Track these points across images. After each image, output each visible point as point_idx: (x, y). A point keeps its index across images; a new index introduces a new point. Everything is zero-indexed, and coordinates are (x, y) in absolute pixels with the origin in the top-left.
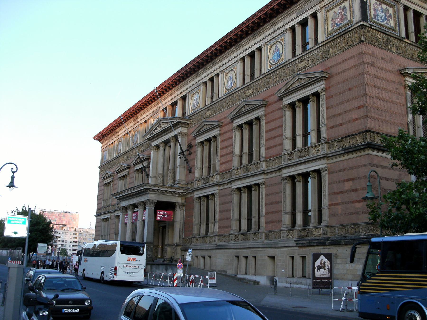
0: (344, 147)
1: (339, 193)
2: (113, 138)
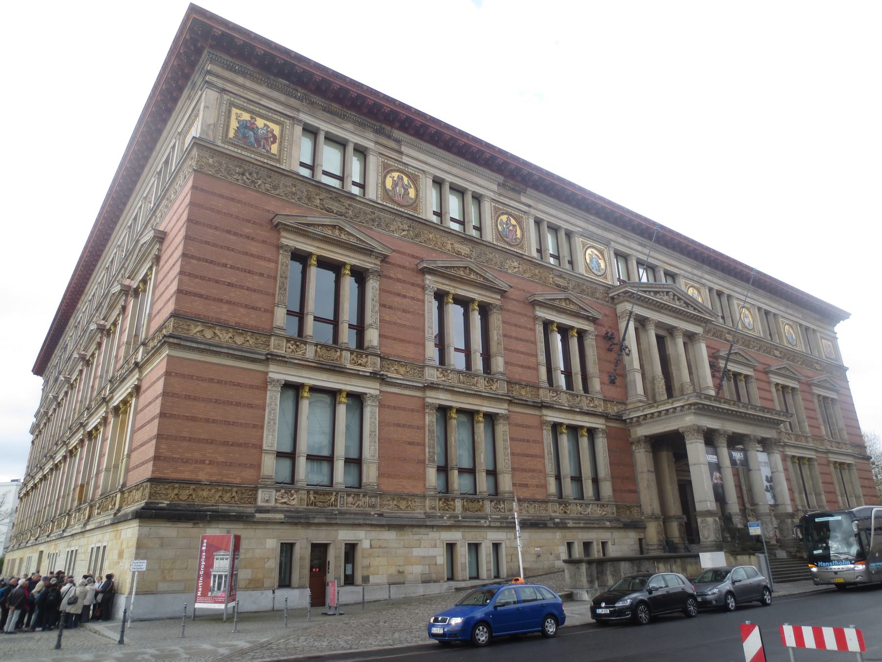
2: (349, 126)
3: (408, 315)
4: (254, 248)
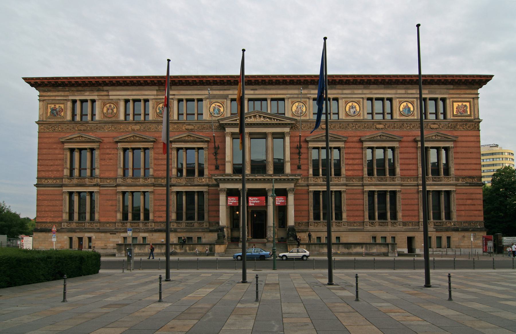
1: (463, 205)
2: (87, 93)
3: (111, 161)
4: (57, 151)
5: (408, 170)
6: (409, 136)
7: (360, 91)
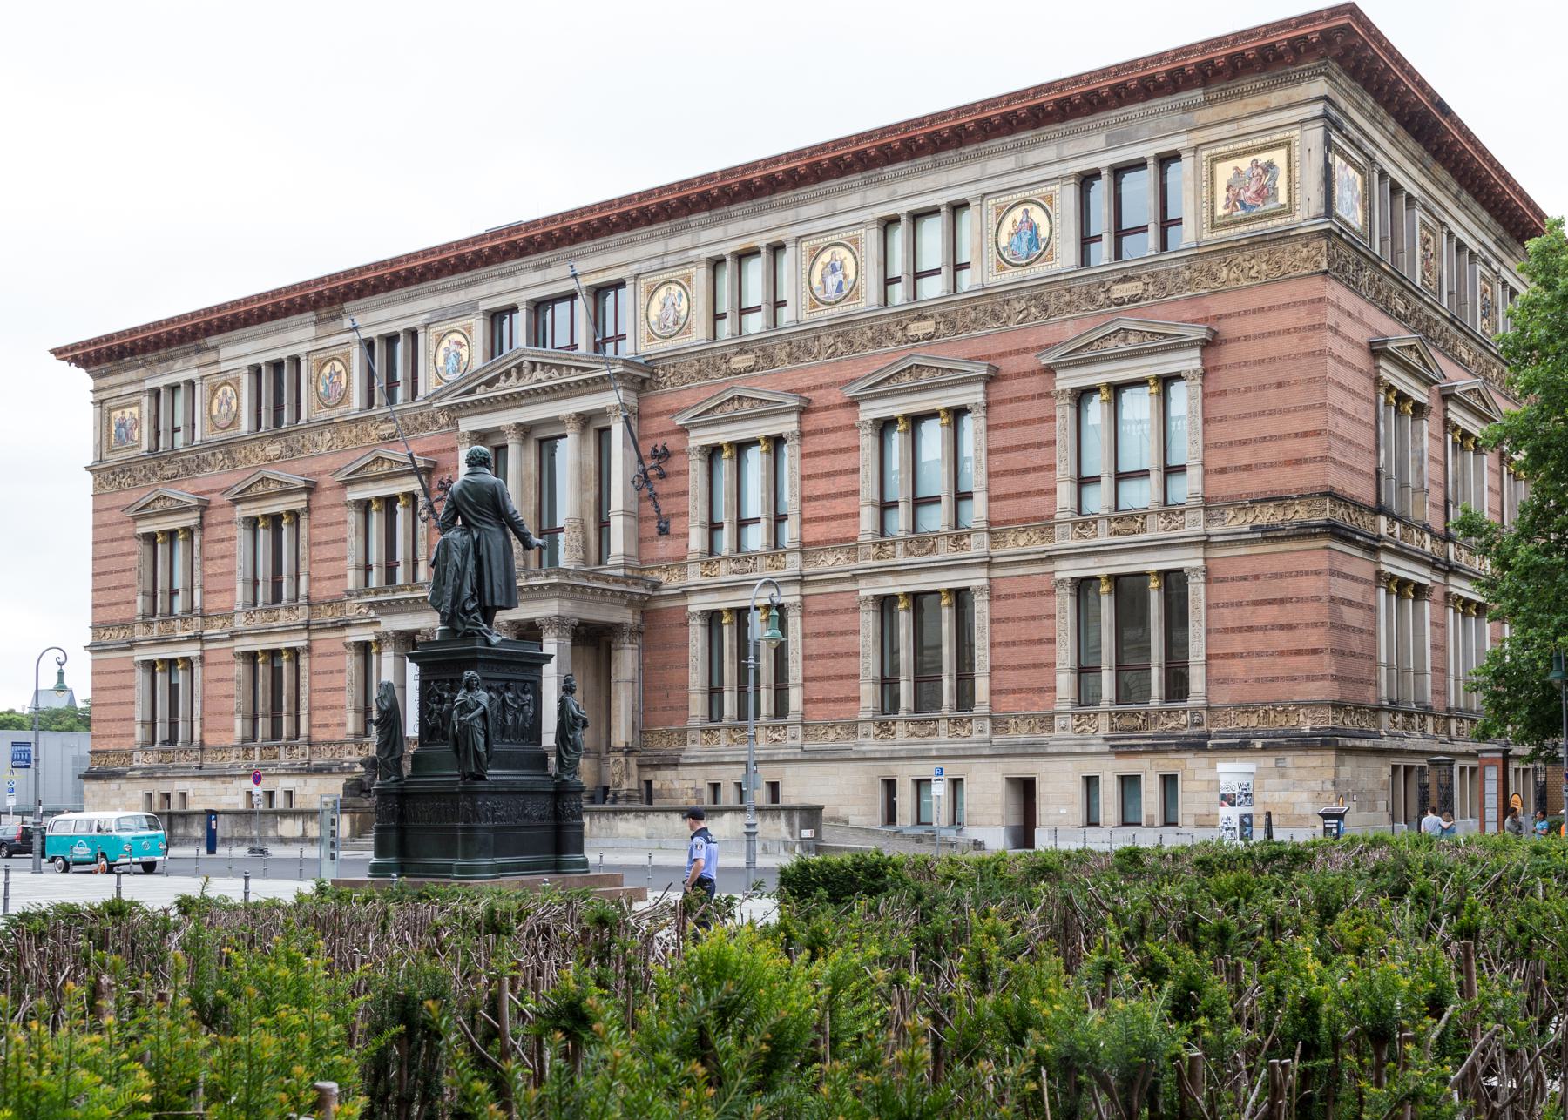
0: (1257, 522)
1: (1240, 630)
2: (178, 365)
5: (1019, 495)
6: (1026, 351)
7: (854, 199)
